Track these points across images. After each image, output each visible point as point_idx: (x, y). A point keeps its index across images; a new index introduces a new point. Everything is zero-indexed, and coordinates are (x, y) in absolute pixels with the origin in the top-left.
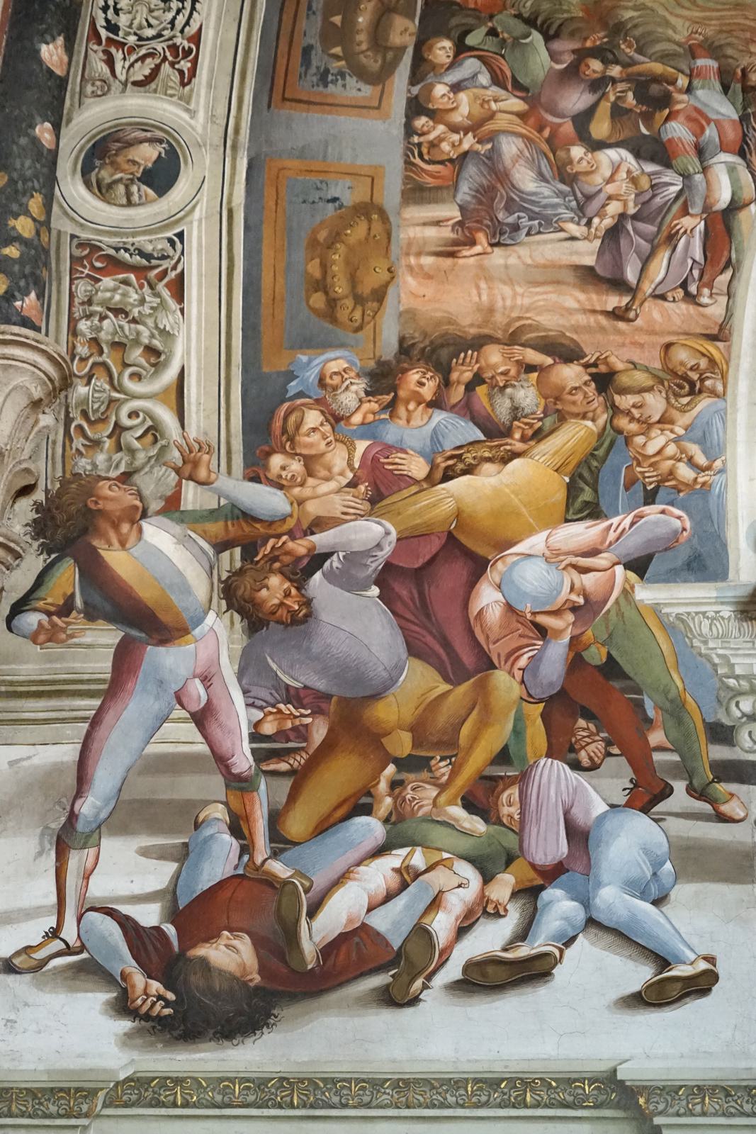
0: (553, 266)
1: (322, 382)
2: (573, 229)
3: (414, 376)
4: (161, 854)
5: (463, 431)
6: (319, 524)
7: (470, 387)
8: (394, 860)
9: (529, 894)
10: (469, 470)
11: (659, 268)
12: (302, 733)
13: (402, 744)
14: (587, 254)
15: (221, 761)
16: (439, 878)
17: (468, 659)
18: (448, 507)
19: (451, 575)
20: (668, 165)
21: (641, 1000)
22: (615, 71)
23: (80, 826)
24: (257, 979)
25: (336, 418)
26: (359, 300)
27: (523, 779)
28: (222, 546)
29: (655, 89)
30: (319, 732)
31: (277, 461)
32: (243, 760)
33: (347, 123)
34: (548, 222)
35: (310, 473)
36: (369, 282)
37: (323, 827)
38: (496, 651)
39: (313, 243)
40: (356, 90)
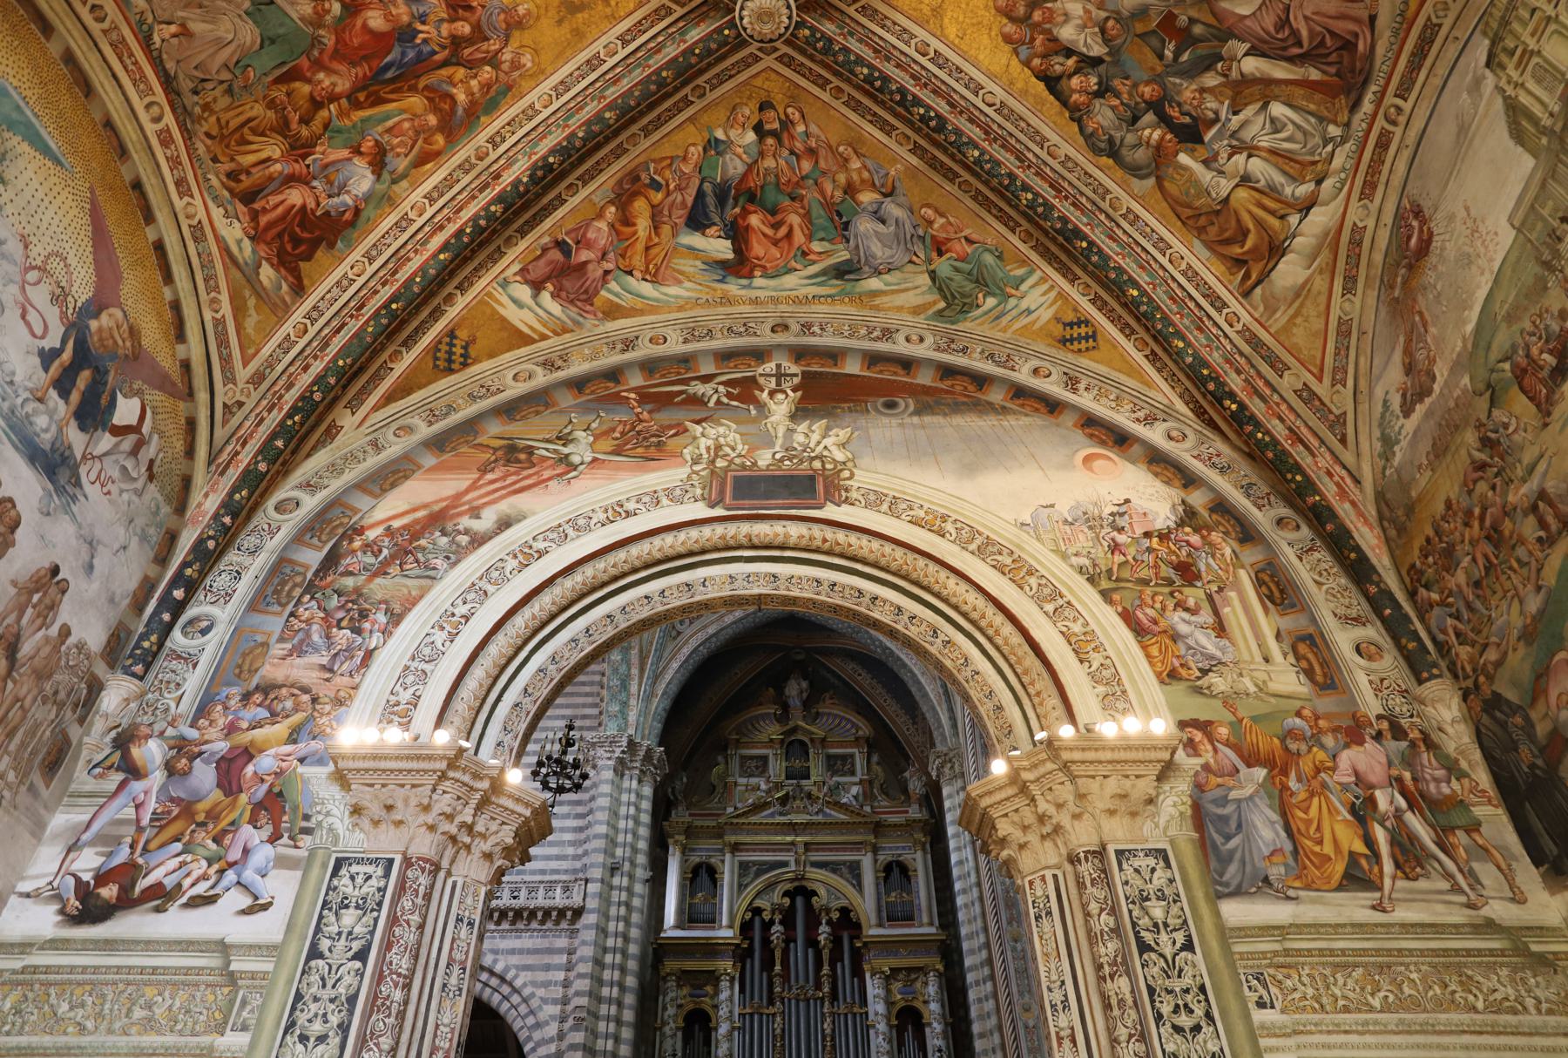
4: (102, 854)
5: (263, 713)
6: (206, 742)
8: (180, 859)
9: (221, 872)
11: (345, 667)
12: (169, 812)
13: (201, 817)
14: (325, 661)
15: (138, 821)
16: (194, 865)
17: (235, 788)
19: (240, 762)
21: (244, 912)
25: (226, 708)
27: (235, 832)
28: (171, 748)
30: (176, 811)
32: (145, 821)
33: (270, 618)
34: (317, 650)
36: (255, 666)
37: (162, 846)
38: (244, 786)
40: (277, 608)
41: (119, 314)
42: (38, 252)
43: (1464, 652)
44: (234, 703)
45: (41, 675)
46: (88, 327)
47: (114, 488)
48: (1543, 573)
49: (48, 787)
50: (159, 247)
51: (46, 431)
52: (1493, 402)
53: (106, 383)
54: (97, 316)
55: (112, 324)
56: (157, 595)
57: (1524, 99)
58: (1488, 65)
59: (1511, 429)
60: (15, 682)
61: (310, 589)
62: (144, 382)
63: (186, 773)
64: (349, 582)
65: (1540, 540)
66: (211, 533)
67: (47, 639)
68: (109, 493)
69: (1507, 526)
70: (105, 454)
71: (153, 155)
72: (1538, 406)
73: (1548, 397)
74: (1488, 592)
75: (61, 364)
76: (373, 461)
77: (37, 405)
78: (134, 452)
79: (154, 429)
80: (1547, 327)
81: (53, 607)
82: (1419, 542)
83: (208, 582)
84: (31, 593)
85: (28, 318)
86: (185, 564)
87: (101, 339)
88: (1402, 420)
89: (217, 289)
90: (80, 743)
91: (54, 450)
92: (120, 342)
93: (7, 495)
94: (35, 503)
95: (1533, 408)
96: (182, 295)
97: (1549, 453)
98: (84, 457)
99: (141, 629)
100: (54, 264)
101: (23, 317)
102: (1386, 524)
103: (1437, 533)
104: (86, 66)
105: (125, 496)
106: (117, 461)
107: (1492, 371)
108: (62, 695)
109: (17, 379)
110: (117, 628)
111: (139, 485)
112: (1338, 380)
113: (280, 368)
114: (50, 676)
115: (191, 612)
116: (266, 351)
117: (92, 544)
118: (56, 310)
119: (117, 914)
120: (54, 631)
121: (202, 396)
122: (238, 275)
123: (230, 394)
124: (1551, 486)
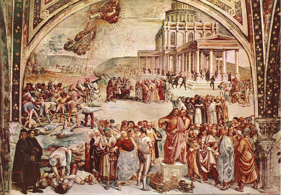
43: (32, 122)
48: (75, 129)
52: (96, 81)
57: (166, 33)
58: (167, 13)
59: (95, 92)
65: (82, 122)
69: (75, 110)
72: (108, 96)
73: (111, 97)
74: (54, 117)
80: (126, 85)
82: (40, 82)
88: (62, 47)
95: (106, 95)
97: (101, 108)
102: (30, 64)
103: (49, 86)
107: (104, 75)
112: (51, 9)
124: (95, 115)
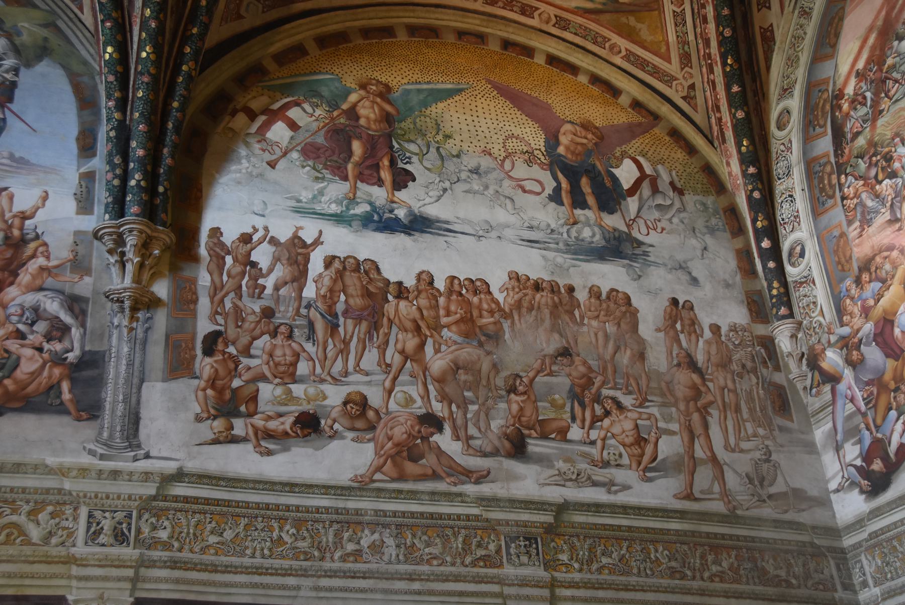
0: (883, 224)
1: (847, 290)
2: (883, 210)
3: (864, 276)
6: (858, 331)
7: (876, 272)
10: (882, 296)
12: (872, 393)
13: (892, 385)
14: (888, 216)
15: (859, 410)
17: (898, 352)
18: (881, 309)
20: (897, 177)
22: (879, 157)
23: (839, 443)
24: (884, 470)
25: (852, 299)
26: (847, 261)
28: (841, 349)
29: (888, 156)
30: (875, 392)
31: (845, 318)
32: (863, 408)
33: (832, 213)
34: (877, 212)
35: (852, 318)
37: (884, 418)
39: (834, 251)
40: (830, 202)
41: (567, 127)
42: (497, 150)
44: (854, 291)
45: (724, 364)
46: (562, 156)
47: (664, 224)
49: (792, 421)
50: (552, 60)
51: (594, 235)
53: (599, 172)
54: (558, 143)
55: (570, 137)
56: (756, 255)
60: (711, 381)
61: (841, 169)
62: (620, 145)
63: (862, 360)
64: (861, 141)
66: (750, 187)
67: (708, 342)
68: (663, 229)
70: (639, 211)
71: (495, 16)
75: (567, 192)
76: (811, 29)
77: (576, 226)
78: (655, 190)
79: (654, 164)
81: (694, 322)
83: (779, 218)
84: (673, 326)
85: (527, 189)
86: (754, 221)
87: (573, 153)
89: (606, 39)
90: (790, 382)
91: (607, 241)
92: (585, 141)
93: (608, 289)
94: (625, 278)
96: (591, 68)
98: (628, 226)
99: (765, 284)
100: (512, 145)
101: (525, 191)
104: (422, 21)
105: (675, 220)
106: (650, 207)
108: (749, 364)
109: (553, 226)
110: (747, 298)
111: (677, 204)
113: (691, 37)
114: (730, 361)
115: (786, 247)
116: (672, 37)
117: (682, 267)
118: (536, 167)
119: (893, 477)
120: (708, 334)
121: (665, 110)
122: (607, 17)
123: (680, 88)
